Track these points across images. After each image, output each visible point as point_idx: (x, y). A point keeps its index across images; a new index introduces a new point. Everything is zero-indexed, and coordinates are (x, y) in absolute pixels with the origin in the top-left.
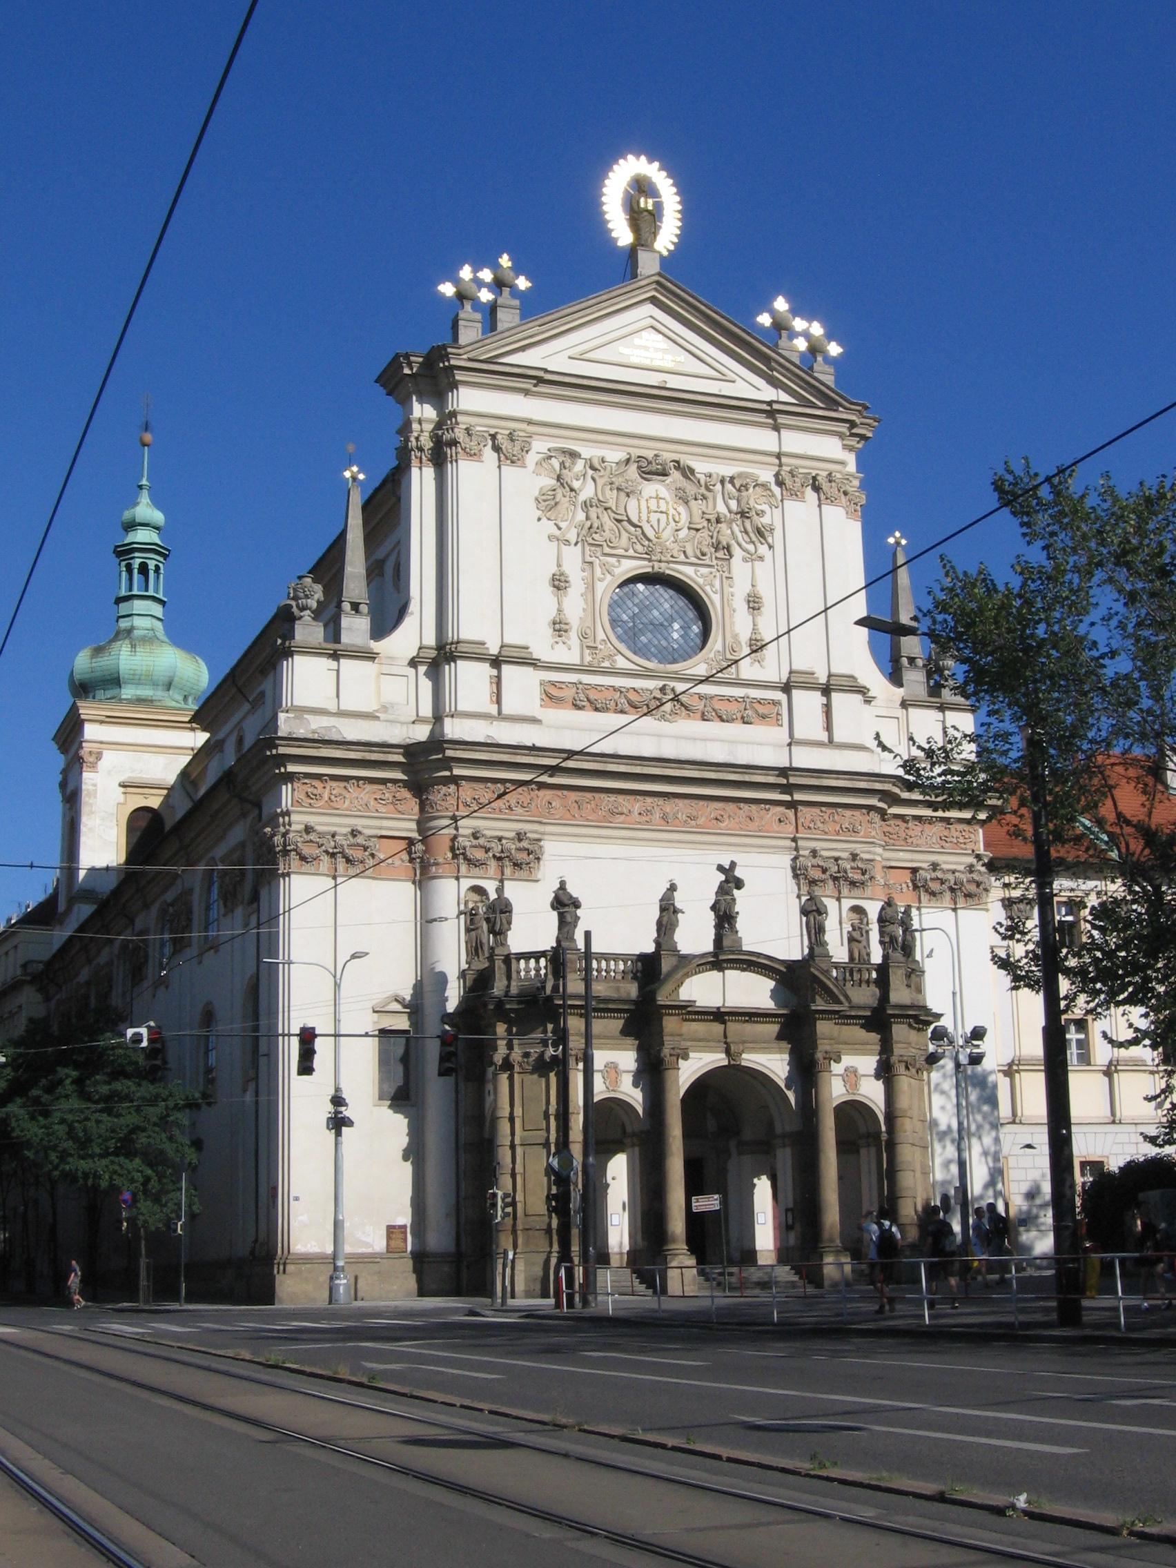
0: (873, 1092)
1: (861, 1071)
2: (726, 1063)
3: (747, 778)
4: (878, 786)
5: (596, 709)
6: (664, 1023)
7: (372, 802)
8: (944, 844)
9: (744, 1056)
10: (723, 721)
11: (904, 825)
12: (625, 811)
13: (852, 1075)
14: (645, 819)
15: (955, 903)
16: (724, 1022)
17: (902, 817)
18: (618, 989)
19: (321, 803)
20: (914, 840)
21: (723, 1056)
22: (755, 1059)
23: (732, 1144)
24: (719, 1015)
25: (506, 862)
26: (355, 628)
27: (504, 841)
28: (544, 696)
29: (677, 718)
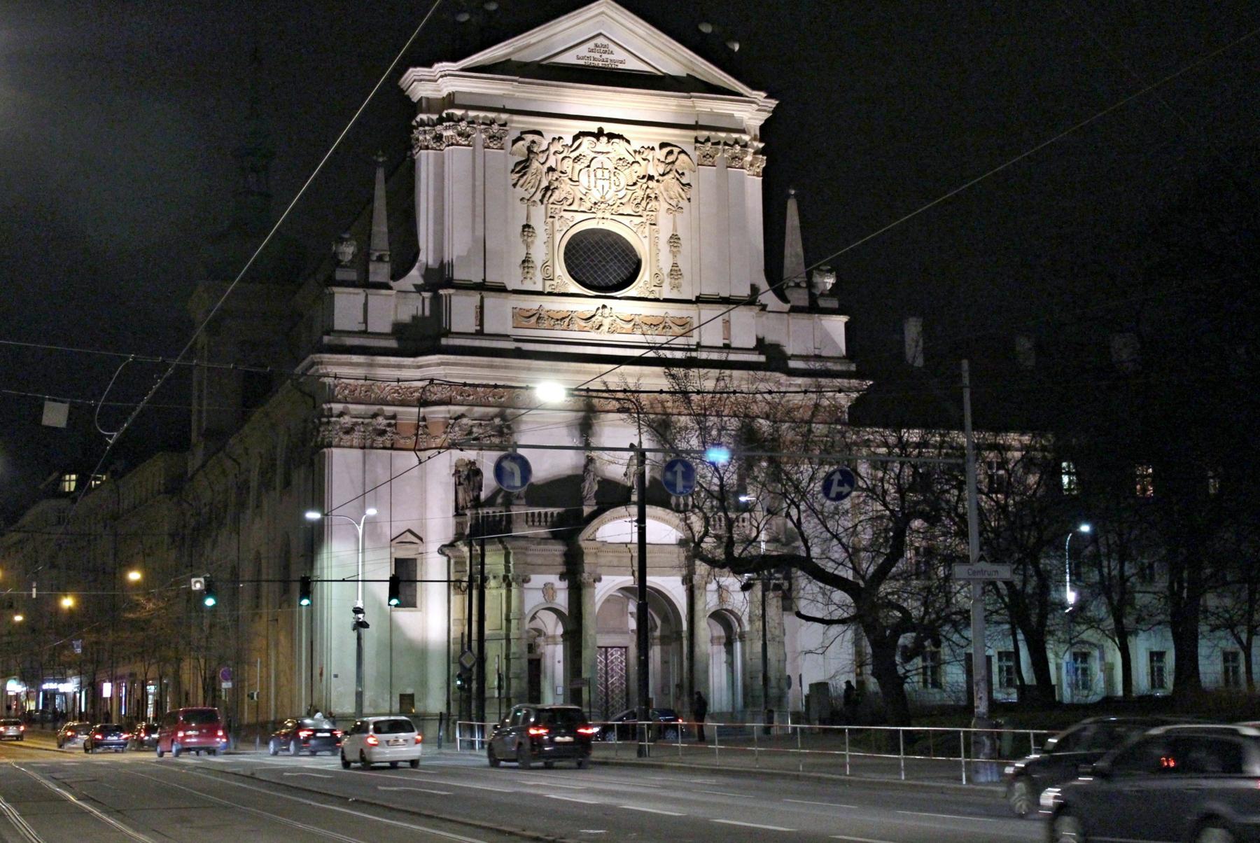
26: (380, 272)
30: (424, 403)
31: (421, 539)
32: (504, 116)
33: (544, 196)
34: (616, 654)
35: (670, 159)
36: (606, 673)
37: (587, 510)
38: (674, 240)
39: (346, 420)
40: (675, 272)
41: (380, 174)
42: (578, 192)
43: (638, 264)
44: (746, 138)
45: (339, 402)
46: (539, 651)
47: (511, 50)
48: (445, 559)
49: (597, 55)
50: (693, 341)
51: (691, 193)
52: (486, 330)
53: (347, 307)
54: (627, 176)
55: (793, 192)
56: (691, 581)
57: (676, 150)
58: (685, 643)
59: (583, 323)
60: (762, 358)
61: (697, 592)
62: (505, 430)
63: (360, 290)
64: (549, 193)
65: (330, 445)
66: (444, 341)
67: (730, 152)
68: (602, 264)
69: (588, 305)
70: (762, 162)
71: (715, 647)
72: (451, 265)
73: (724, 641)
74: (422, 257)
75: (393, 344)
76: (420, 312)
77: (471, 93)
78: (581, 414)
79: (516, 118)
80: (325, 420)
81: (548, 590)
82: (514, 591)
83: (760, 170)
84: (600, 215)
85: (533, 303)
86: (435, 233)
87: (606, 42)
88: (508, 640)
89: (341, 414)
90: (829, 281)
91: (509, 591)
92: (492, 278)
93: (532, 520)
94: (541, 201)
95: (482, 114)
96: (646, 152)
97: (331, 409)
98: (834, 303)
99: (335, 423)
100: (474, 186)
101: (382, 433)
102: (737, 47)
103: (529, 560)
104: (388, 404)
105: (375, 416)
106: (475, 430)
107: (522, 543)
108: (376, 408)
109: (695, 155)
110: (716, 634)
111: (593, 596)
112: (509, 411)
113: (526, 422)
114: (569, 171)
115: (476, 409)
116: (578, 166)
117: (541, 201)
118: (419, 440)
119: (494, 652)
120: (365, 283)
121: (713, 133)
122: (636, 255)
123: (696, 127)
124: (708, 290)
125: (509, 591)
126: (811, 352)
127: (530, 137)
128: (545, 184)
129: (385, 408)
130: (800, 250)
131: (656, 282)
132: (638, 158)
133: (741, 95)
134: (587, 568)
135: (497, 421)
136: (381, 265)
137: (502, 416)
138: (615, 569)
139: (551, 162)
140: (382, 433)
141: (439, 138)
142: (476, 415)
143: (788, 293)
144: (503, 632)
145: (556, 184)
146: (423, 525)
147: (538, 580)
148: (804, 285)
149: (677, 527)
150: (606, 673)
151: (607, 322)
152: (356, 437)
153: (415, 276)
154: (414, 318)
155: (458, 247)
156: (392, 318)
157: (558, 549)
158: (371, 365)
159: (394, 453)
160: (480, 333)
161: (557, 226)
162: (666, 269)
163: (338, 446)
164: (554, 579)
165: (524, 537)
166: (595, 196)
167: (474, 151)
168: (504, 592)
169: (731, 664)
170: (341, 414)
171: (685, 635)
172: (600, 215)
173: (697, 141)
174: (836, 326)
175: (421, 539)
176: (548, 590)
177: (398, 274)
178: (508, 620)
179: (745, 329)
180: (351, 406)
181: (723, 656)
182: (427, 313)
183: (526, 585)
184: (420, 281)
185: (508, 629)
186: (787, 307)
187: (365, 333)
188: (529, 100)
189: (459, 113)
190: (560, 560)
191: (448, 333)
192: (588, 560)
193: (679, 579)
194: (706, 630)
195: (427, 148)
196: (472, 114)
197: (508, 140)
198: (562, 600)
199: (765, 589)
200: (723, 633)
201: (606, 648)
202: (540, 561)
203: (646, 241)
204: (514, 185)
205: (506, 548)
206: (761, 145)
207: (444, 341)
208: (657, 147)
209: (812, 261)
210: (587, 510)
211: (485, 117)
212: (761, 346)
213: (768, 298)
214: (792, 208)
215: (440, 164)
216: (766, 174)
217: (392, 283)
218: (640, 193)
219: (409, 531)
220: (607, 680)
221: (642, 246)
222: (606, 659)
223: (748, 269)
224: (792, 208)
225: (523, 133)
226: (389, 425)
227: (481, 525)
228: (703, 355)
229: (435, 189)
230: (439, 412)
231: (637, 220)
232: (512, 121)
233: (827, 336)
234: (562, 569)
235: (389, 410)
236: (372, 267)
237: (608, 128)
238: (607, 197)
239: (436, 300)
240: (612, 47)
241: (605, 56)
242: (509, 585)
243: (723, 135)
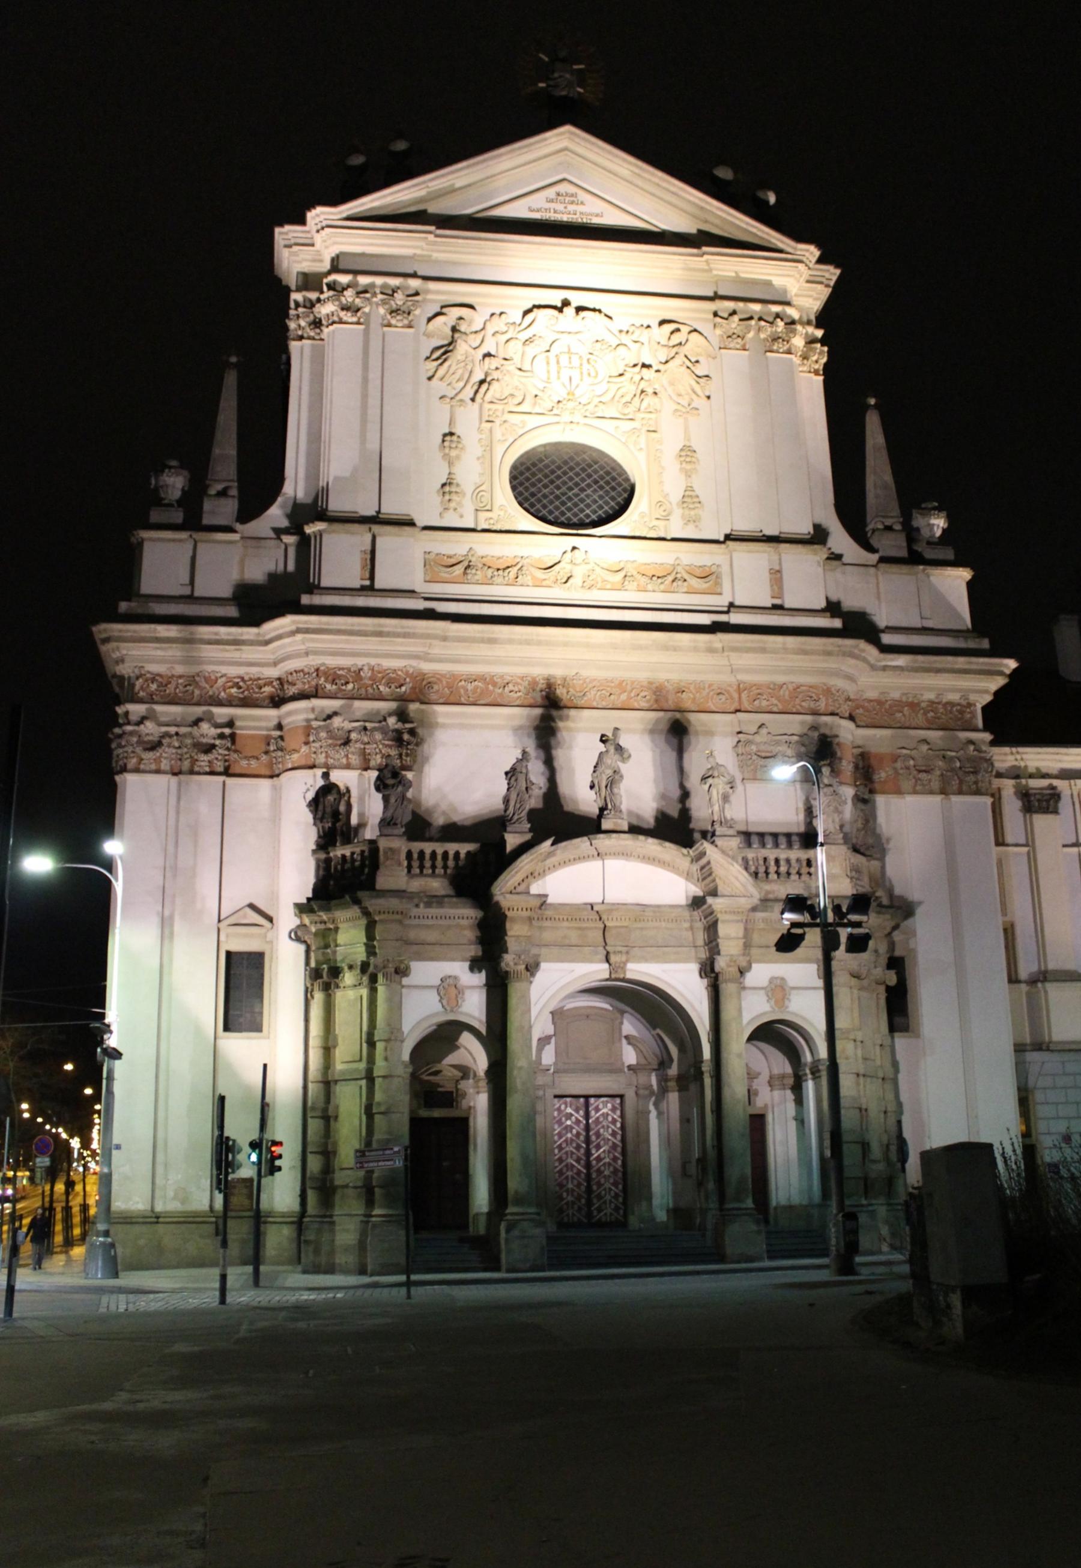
0: (807, 1009)
9: (630, 966)
13: (778, 990)
30: (277, 702)
31: (270, 919)
32: (414, 283)
33: (476, 392)
34: (605, 1108)
35: (676, 338)
36: (588, 1141)
37: (512, 841)
38: (687, 453)
39: (149, 727)
40: (690, 499)
41: (231, 380)
42: (532, 385)
43: (630, 493)
44: (793, 313)
45: (141, 701)
46: (464, 1104)
47: (423, 193)
48: (302, 948)
49: (560, 207)
50: (722, 601)
51: (711, 388)
52: (378, 585)
53: (164, 561)
54: (611, 362)
55: (872, 401)
56: (712, 970)
57: (685, 329)
58: (708, 1081)
59: (540, 575)
60: (837, 623)
61: (728, 989)
62: (406, 737)
63: (184, 535)
64: (485, 387)
65: (124, 770)
66: (305, 600)
67: (767, 331)
68: (572, 491)
69: (550, 545)
70: (820, 356)
71: (776, 1093)
72: (326, 491)
73: (791, 1081)
74: (288, 489)
75: (232, 612)
76: (281, 567)
77: (363, 255)
78: (538, 711)
79: (432, 286)
80: (117, 730)
81: (448, 988)
82: (381, 990)
83: (820, 366)
84: (566, 417)
85: (457, 546)
86: (309, 454)
87: (572, 189)
88: (370, 1078)
89: (141, 721)
90: (939, 523)
91: (373, 991)
92: (390, 508)
93: (417, 864)
94: (473, 400)
95: (379, 281)
96: (638, 332)
97: (127, 713)
98: (949, 554)
99: (131, 733)
100: (365, 380)
101: (209, 749)
102: (772, 199)
103: (412, 935)
104: (220, 704)
105: (196, 722)
106: (353, 736)
107: (394, 903)
108: (199, 710)
109: (715, 335)
110: (776, 1071)
111: (526, 998)
112: (413, 707)
113: (444, 726)
114: (517, 359)
115: (357, 704)
116: (531, 350)
117: (473, 400)
118: (271, 759)
119: (349, 1102)
120: (193, 522)
121: (741, 305)
122: (627, 479)
123: (716, 297)
124: (744, 526)
125: (373, 991)
126: (917, 623)
127: (456, 312)
128: (479, 376)
129: (216, 710)
130: (888, 477)
131: (660, 513)
132: (625, 339)
133: (781, 251)
134: (512, 944)
135: (392, 721)
136: (223, 501)
137: (402, 715)
138: (568, 950)
139: (489, 346)
140: (209, 749)
141: (317, 324)
142: (358, 715)
143: (874, 542)
144: (363, 1065)
145: (495, 375)
146: (274, 896)
147: (425, 972)
148: (898, 527)
149: (688, 876)
150: (588, 1141)
151: (579, 573)
152: (166, 756)
153: (276, 514)
154: (272, 577)
155: (340, 462)
156: (235, 576)
157: (466, 915)
158: (189, 641)
159: (230, 781)
160: (370, 589)
161: (498, 434)
162: (676, 496)
163: (137, 770)
164: (459, 969)
165: (399, 893)
166: (558, 391)
167: (367, 332)
168: (364, 992)
169: (801, 1121)
170: (141, 721)
171: (707, 1067)
172: (566, 417)
173: (715, 314)
174: (954, 583)
175: (270, 919)
176: (448, 988)
177: (250, 511)
178: (371, 1044)
179: (807, 582)
180: (159, 708)
181: (791, 1108)
182: (291, 567)
183: (405, 981)
184: (285, 523)
185: (371, 1060)
186: (874, 558)
187: (190, 598)
188: (455, 263)
189: (344, 279)
190: (470, 934)
191: (313, 588)
192: (515, 931)
193: (694, 968)
194: (742, 1058)
195: (301, 338)
196: (364, 280)
197: (420, 314)
198: (474, 1006)
199: (830, 945)
200: (788, 1069)
201: (587, 1097)
202: (431, 936)
203: (642, 457)
204: (430, 379)
205: (366, 913)
206: (819, 333)
207: (305, 600)
208: (654, 324)
209: (911, 498)
210: (512, 841)
211: (385, 286)
212: (833, 608)
213: (840, 540)
214: (873, 424)
215: (319, 360)
216: (830, 373)
217: (238, 526)
218: (632, 389)
219: (252, 906)
220: (588, 1153)
221: (634, 464)
222: (587, 1116)
223: (810, 500)
224: (873, 424)
225: (442, 307)
226: (222, 736)
227: (343, 881)
228: (735, 618)
229: (311, 394)
230: (297, 713)
231: (628, 425)
232: (428, 291)
233: (940, 600)
234: (475, 950)
235: (222, 713)
236: (207, 505)
237: (577, 299)
238: (578, 393)
239: (305, 543)
240: (582, 196)
241: (571, 208)
242: (373, 979)
243: (756, 307)
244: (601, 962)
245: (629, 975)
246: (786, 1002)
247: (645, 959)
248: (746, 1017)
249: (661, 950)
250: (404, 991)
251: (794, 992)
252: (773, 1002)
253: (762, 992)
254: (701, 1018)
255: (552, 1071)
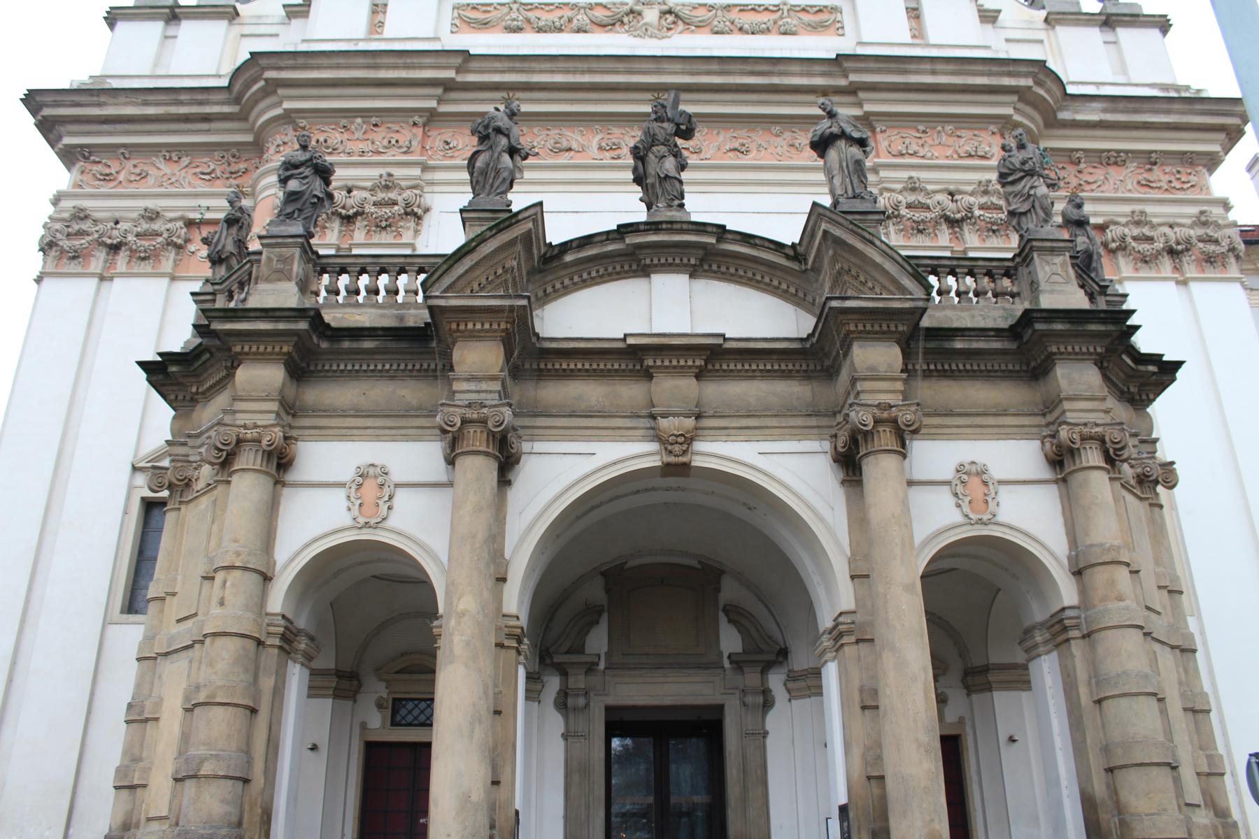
0: (1030, 515)
1: (997, 473)
2: (654, 462)
3: (776, 80)
4: (1007, 81)
5: (540, 30)
6: (456, 355)
7: (190, 177)
8: (1147, 190)
9: (699, 446)
10: (747, 33)
11: (1072, 169)
12: (574, 146)
14: (607, 154)
15: (1182, 274)
16: (648, 375)
17: (1072, 157)
18: (401, 318)
19: (115, 183)
20: (1094, 187)
21: (653, 446)
22: (723, 453)
23: (776, 681)
24: (637, 358)
25: (360, 223)
27: (354, 193)
28: (457, 21)
29: (670, 33)
244: (644, 439)
245: (698, 462)
246: (992, 505)
247: (725, 433)
248: (921, 532)
249: (753, 422)
250: (286, 491)
251: (1002, 489)
252: (966, 509)
253: (947, 488)
254: (833, 534)
255: (602, 666)
